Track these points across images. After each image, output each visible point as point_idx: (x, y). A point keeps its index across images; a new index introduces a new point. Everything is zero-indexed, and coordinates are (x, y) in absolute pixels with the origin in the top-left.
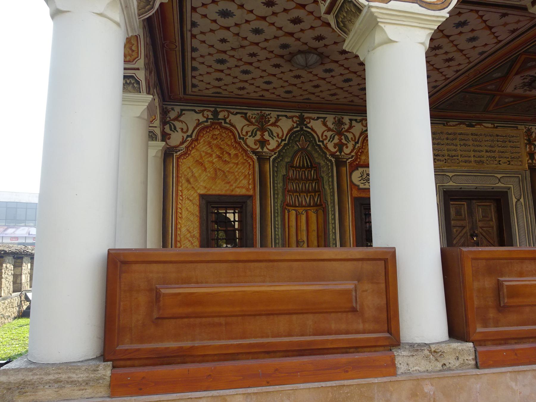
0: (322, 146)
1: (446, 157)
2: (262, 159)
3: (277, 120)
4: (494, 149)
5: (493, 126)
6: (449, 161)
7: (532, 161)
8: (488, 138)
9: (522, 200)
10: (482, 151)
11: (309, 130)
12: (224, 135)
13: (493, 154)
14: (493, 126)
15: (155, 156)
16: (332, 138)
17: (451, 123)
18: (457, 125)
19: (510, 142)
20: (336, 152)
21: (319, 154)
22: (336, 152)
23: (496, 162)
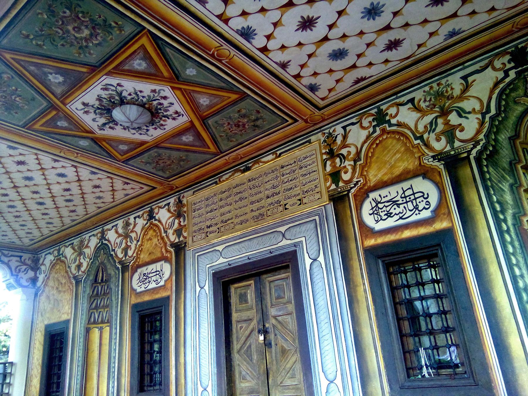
0: (114, 255)
1: (218, 226)
2: (78, 282)
3: (89, 241)
4: (277, 190)
5: (275, 155)
6: (222, 229)
7: (337, 185)
8: (270, 177)
9: (321, 259)
10: (261, 199)
11: (106, 242)
12: (61, 267)
13: (276, 198)
14: (275, 155)
15: (21, 300)
16: (121, 243)
17: (224, 178)
18: (230, 176)
19: (301, 168)
20: (122, 258)
21: (111, 264)
22: (122, 258)
23: (281, 208)
